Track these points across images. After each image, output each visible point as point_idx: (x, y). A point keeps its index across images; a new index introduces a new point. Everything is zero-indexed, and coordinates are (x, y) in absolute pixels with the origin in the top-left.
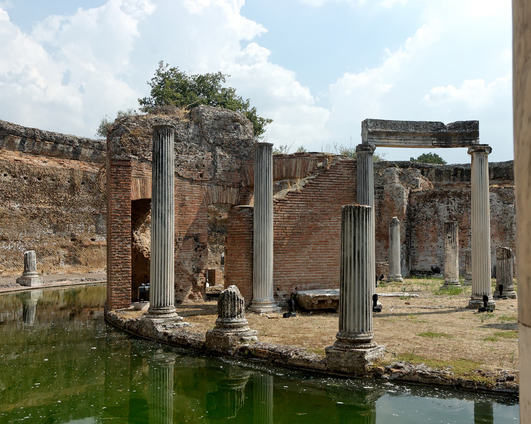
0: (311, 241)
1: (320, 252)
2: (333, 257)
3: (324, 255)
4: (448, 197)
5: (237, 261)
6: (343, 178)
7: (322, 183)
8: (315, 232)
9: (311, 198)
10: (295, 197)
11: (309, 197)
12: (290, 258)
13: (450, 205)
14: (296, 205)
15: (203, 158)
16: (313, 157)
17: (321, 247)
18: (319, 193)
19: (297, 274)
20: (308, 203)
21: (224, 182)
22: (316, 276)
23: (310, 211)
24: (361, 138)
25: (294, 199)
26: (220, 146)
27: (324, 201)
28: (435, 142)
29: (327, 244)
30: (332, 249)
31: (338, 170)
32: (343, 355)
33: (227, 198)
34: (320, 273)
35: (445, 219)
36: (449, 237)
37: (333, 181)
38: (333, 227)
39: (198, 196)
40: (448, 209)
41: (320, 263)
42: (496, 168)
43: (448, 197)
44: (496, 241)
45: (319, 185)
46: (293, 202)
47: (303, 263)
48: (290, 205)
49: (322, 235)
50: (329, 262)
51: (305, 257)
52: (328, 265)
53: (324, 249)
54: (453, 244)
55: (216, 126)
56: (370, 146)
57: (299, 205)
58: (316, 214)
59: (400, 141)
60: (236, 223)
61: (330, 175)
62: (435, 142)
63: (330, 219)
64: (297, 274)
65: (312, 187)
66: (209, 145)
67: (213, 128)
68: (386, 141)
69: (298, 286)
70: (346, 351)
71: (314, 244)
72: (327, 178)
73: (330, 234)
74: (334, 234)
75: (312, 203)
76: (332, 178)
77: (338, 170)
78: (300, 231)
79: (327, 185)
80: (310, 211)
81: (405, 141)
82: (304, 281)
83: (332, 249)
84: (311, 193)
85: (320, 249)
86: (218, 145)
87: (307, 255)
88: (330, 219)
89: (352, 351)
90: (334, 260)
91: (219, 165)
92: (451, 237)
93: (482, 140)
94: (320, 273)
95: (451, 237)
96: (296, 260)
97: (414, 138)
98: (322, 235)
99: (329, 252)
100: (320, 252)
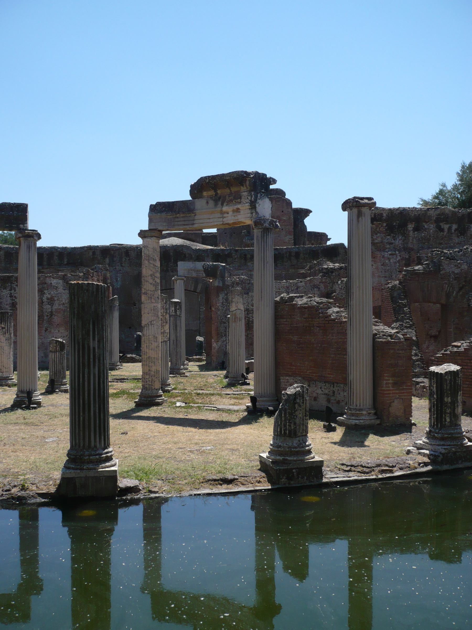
4: (11, 283)
13: (13, 291)
35: (7, 307)
36: (3, 328)
40: (11, 296)
42: (70, 253)
43: (11, 283)
44: (61, 331)
54: (7, 335)
92: (5, 328)
93: (32, 225)
95: (5, 328)
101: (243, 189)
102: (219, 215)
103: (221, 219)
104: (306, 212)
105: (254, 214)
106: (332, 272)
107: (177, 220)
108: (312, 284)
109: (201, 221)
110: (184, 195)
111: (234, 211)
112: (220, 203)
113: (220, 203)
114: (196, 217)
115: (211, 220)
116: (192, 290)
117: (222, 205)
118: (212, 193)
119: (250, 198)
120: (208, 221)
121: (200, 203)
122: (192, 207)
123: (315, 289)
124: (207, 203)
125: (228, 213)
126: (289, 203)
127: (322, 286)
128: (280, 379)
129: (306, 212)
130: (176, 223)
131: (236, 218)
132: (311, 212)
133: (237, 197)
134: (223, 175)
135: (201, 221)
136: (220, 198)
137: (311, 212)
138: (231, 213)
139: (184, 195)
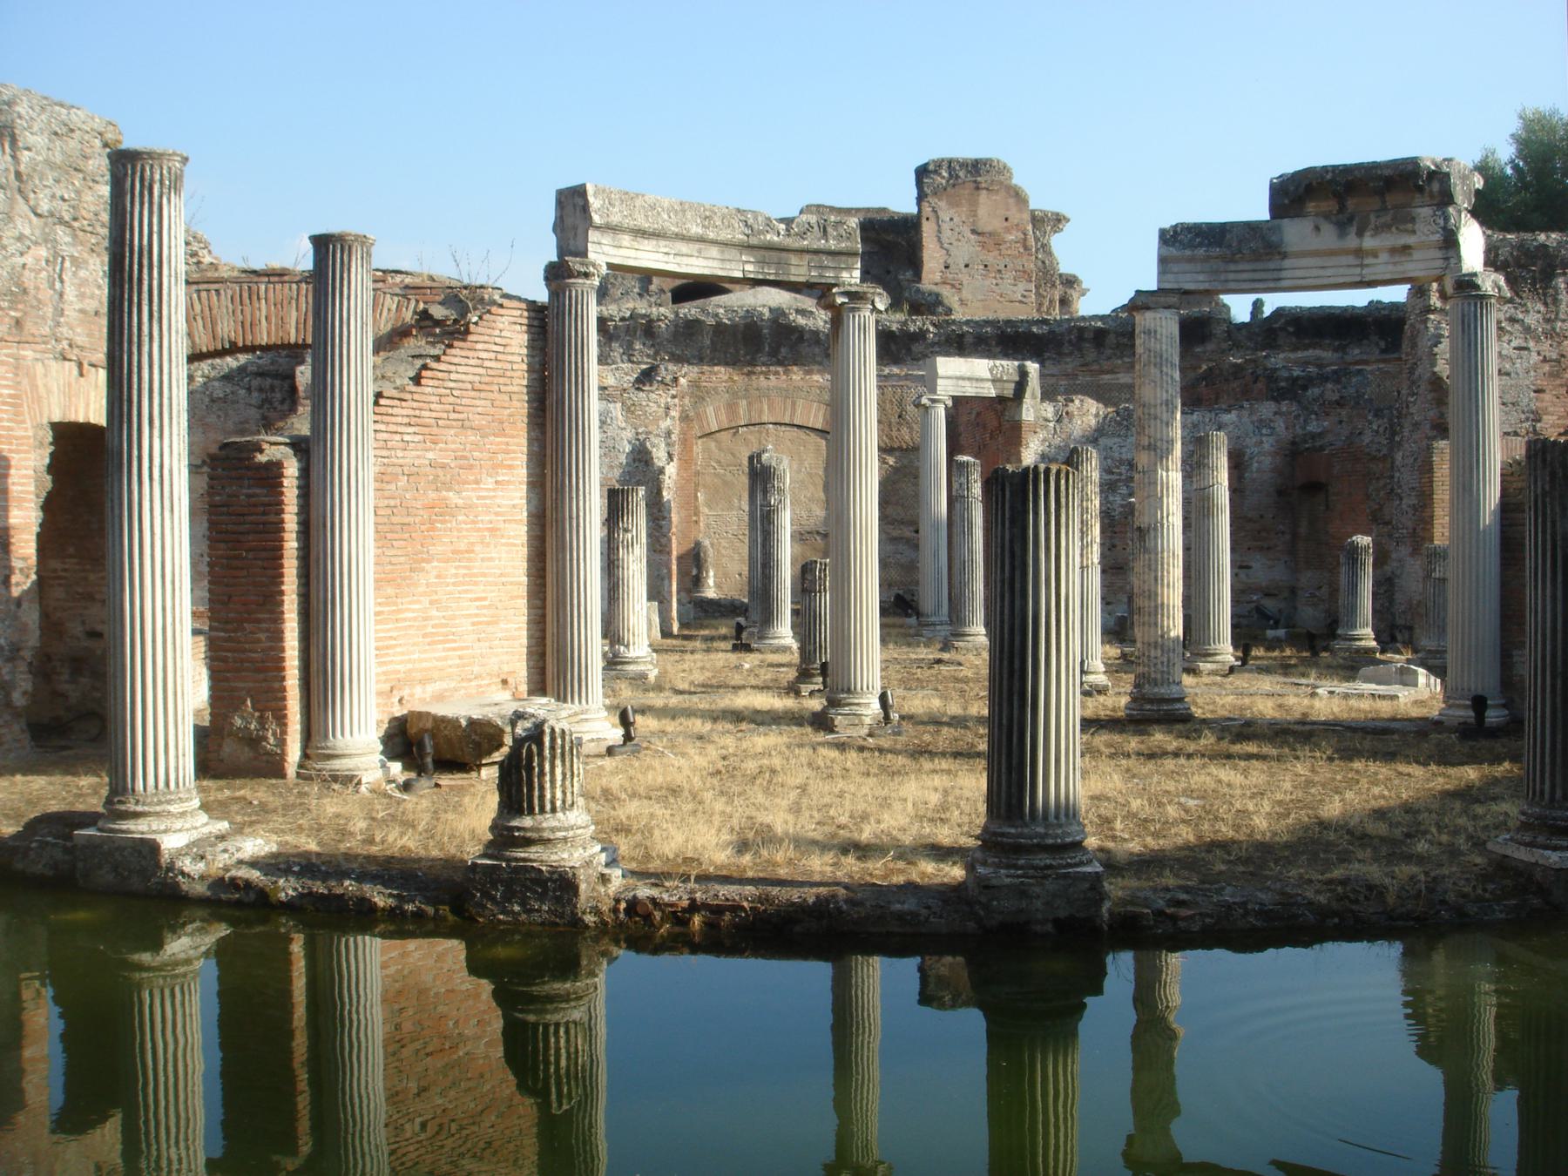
0: (433, 550)
1: (454, 584)
2: (485, 599)
3: (466, 591)
5: (259, 621)
6: (510, 358)
7: (460, 369)
8: (442, 522)
9: (434, 415)
10: (395, 411)
11: (427, 414)
12: (387, 604)
14: (398, 437)
15: (24, 266)
16: (395, 285)
17: (457, 568)
18: (451, 399)
19: (402, 654)
20: (426, 430)
21: (82, 348)
22: (445, 658)
23: (431, 455)
24: (553, 239)
25: (393, 419)
26: (67, 224)
27: (463, 426)
28: (749, 267)
29: (469, 560)
30: (484, 575)
31: (497, 333)
32: (1037, 890)
33: (87, 405)
34: (454, 649)
37: (487, 364)
38: (486, 505)
39: (10, 396)
41: (453, 618)
45: (453, 376)
46: (392, 428)
47: (415, 619)
48: (385, 436)
49: (459, 530)
50: (477, 615)
51: (419, 602)
52: (474, 624)
53: (464, 575)
55: (58, 158)
56: (594, 265)
57: (406, 438)
58: (443, 467)
59: (666, 258)
60: (249, 496)
61: (479, 346)
62: (749, 267)
63: (477, 482)
64: (402, 654)
65: (436, 383)
66: (34, 219)
67: (47, 162)
68: (632, 253)
69: (406, 692)
70: (1045, 877)
71: (439, 561)
72: (471, 354)
73: (479, 530)
74: (489, 529)
75: (435, 430)
76: (484, 355)
77: (497, 333)
78: (406, 520)
79: (470, 378)
80: (431, 455)
81: (678, 259)
82: (418, 676)
83: (484, 575)
84: (434, 399)
85: (456, 575)
86: (61, 221)
87: (424, 594)
88: (477, 482)
89: (1066, 876)
90: (490, 606)
91: (70, 293)
94: (454, 649)
96: (399, 611)
97: (700, 251)
98: (459, 530)
99: (476, 584)
100: (454, 584)
101: (1418, 199)
102: (1351, 260)
103: (1358, 270)
104: (1058, 221)
105: (1453, 261)
106: (1305, 388)
107: (1232, 267)
108: (1255, 418)
109: (1299, 273)
110: (1257, 209)
111: (1393, 251)
112: (1353, 230)
113: (1353, 230)
114: (1287, 263)
115: (1329, 272)
116: (819, 426)
117: (1360, 234)
118: (1331, 205)
119: (1441, 222)
120: (1321, 272)
121: (1296, 233)
122: (1274, 238)
123: (1264, 431)
124: (1317, 228)
125: (1376, 256)
126: (1019, 197)
127: (1280, 425)
128: (1510, 656)
129: (1058, 221)
130: (1231, 276)
131: (1400, 268)
132: (1068, 220)
133: (1403, 220)
134: (1375, 166)
135: (1299, 273)
136: (1351, 220)
137: (1068, 220)
138: (1384, 257)
139: (1257, 209)
